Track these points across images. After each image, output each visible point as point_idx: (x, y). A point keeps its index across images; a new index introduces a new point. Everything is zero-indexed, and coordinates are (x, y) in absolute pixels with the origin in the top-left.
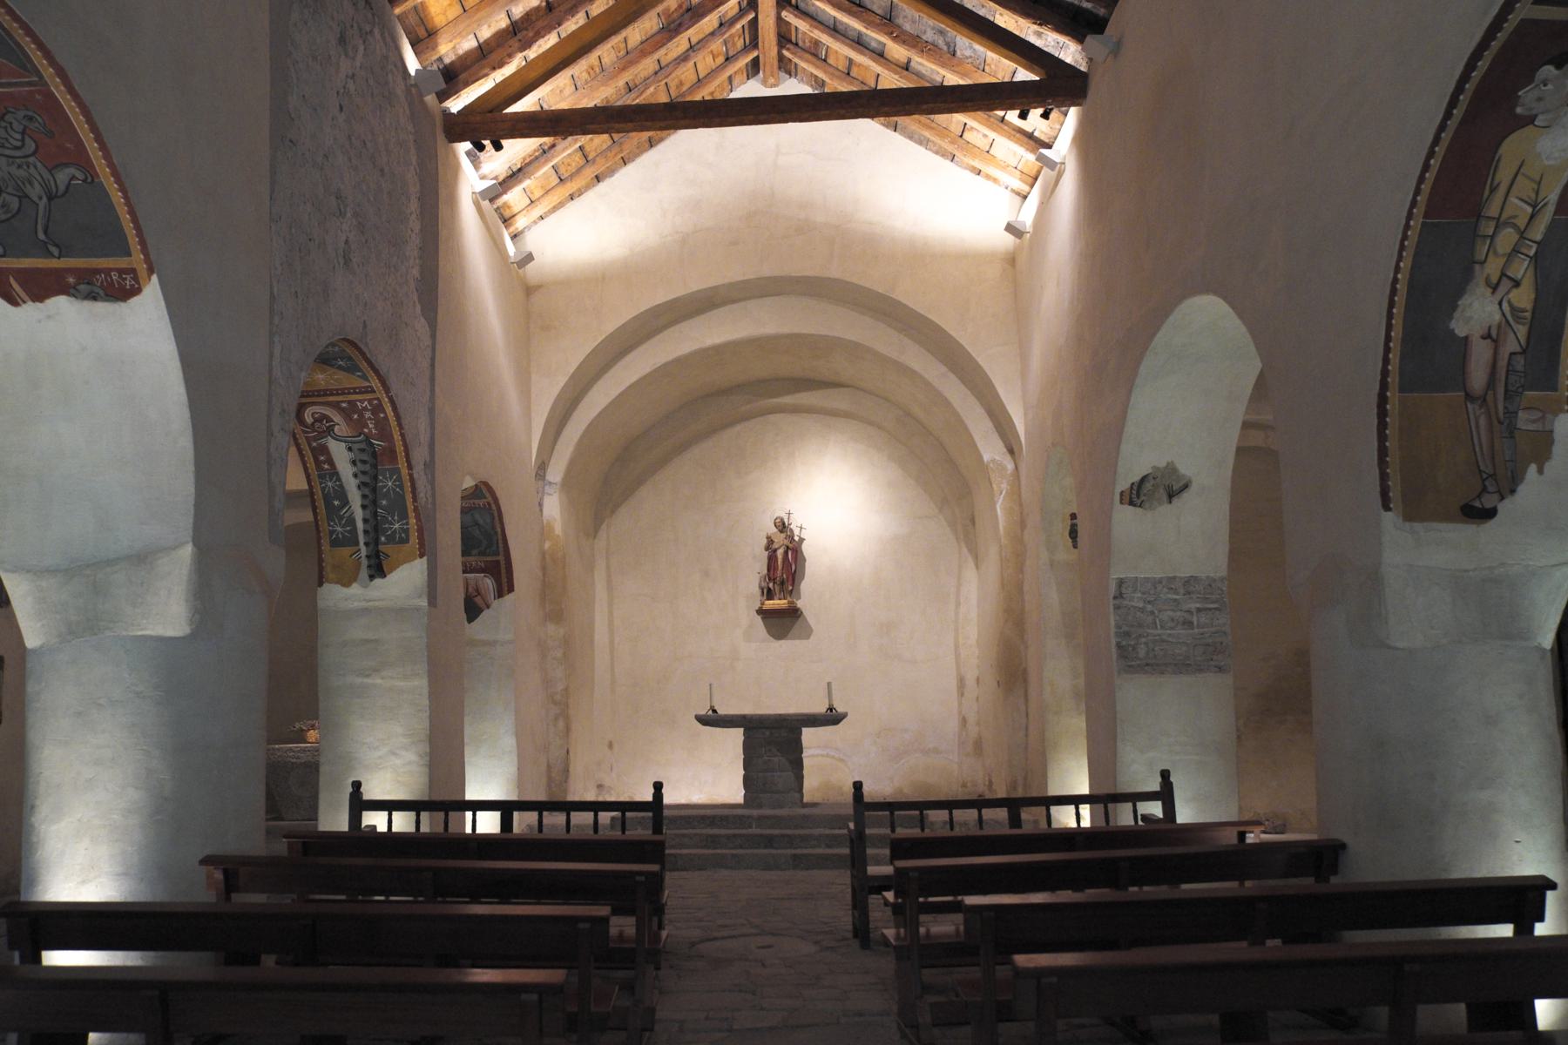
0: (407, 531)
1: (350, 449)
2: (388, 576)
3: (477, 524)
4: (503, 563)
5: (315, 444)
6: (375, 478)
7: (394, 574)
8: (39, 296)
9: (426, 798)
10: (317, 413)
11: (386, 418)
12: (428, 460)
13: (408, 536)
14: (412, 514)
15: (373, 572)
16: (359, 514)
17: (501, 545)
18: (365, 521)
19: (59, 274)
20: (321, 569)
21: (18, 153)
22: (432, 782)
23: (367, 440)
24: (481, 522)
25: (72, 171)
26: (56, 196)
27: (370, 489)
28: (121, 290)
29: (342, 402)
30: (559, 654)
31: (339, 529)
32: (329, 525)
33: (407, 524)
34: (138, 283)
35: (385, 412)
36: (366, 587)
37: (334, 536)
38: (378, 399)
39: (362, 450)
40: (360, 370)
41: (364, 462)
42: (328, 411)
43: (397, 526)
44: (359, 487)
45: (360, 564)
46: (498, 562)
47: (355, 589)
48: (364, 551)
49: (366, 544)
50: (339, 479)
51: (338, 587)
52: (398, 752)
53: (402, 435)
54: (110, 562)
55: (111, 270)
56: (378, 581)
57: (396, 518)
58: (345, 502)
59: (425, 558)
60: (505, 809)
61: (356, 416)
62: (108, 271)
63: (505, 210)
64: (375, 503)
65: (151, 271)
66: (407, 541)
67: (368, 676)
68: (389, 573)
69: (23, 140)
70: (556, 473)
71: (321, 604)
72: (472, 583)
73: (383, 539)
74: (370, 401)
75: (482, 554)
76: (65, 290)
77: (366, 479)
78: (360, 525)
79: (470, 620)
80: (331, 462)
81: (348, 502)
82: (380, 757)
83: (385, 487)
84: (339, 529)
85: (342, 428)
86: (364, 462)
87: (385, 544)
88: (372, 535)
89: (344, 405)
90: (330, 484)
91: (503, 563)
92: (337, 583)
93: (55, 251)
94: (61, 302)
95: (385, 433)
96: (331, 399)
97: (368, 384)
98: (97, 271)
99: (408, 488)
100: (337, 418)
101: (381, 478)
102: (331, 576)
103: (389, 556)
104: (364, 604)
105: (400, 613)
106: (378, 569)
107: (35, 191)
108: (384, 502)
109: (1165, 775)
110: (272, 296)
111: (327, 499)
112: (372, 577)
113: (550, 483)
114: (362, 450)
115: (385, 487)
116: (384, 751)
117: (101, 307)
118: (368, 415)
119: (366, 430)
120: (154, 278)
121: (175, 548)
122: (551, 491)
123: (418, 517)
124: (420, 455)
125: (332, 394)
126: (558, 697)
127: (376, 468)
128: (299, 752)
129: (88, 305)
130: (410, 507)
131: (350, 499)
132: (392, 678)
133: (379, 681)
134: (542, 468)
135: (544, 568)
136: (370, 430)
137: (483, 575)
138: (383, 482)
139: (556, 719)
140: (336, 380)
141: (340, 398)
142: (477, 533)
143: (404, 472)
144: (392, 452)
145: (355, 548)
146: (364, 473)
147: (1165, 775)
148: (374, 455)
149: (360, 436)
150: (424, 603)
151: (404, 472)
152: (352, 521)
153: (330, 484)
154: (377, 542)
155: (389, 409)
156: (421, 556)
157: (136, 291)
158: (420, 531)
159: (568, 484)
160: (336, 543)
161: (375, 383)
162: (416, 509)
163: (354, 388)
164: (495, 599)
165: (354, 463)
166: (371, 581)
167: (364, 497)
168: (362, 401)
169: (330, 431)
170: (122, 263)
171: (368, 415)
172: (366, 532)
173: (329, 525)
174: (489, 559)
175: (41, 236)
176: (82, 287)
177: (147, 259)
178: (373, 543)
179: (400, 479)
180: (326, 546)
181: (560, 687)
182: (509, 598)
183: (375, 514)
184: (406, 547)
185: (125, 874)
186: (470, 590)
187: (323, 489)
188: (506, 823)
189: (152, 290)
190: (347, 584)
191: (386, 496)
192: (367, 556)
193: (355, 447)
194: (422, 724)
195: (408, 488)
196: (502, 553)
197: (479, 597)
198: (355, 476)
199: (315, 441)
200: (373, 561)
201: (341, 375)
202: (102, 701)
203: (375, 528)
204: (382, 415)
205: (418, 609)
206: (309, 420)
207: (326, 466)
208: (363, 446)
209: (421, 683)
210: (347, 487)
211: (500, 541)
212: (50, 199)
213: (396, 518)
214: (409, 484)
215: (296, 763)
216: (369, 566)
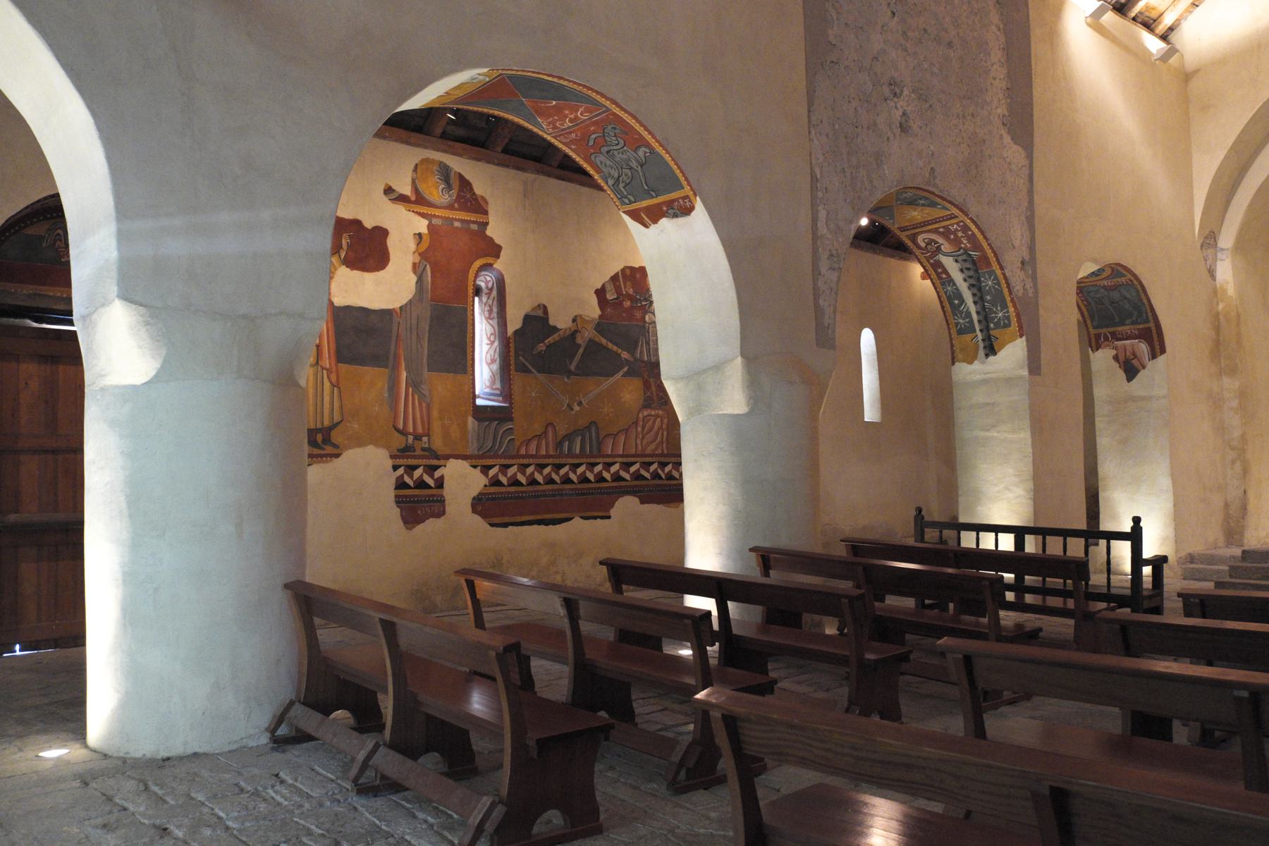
0: (1008, 318)
1: (956, 261)
2: (998, 354)
3: (1125, 298)
4: (1154, 329)
5: (932, 261)
6: (979, 280)
7: (1001, 352)
8: (655, 221)
9: (1032, 525)
10: (926, 239)
11: (973, 234)
12: (1027, 258)
13: (1009, 321)
14: (1010, 305)
15: (987, 352)
17: (1150, 314)
18: (978, 313)
19: (659, 205)
20: (953, 352)
22: (1036, 513)
23: (966, 252)
24: (1128, 296)
25: (643, 149)
26: (644, 165)
27: (977, 287)
28: (687, 211)
29: (940, 228)
30: (1235, 403)
31: (961, 321)
32: (955, 319)
33: (1008, 312)
34: (692, 203)
35: (970, 230)
36: (983, 363)
37: (959, 327)
38: (962, 221)
39: (965, 260)
40: (940, 204)
41: (968, 269)
42: (934, 237)
43: (1000, 315)
44: (969, 288)
45: (978, 346)
46: (1149, 329)
47: (976, 365)
48: (980, 337)
49: (981, 331)
50: (955, 284)
52: (1010, 487)
53: (989, 245)
54: (705, 371)
55: (680, 198)
56: (991, 358)
57: (999, 308)
58: (962, 301)
59: (1024, 338)
60: (1019, 533)
61: (952, 237)
62: (676, 200)
63: (1150, 13)
64: (982, 298)
65: (695, 195)
66: (1009, 325)
67: (988, 430)
68: (999, 351)
69: (617, 140)
70: (1227, 239)
71: (955, 378)
73: (992, 325)
74: (957, 224)
75: (1133, 323)
76: (664, 215)
77: (973, 282)
78: (975, 317)
79: (1129, 379)
81: (963, 301)
82: (998, 492)
83: (987, 285)
84: (961, 321)
85: (946, 247)
86: (968, 269)
87: (994, 329)
88: (984, 323)
89: (941, 230)
90: (949, 288)
91: (1154, 329)
92: (964, 361)
94: (664, 222)
95: (977, 246)
96: (930, 227)
97: (950, 213)
98: (672, 201)
100: (941, 240)
101: (983, 279)
102: (960, 356)
103: (997, 339)
104: (984, 377)
105: (1009, 381)
106: (991, 350)
107: (634, 164)
108: (988, 298)
109: (1137, 520)
110: (814, 179)
111: (950, 299)
112: (987, 356)
113: (1222, 250)
114: (965, 260)
115: (987, 285)
116: (1001, 486)
117: (681, 220)
118: (960, 234)
119: (963, 246)
120: (698, 198)
121: (733, 359)
122: (1224, 257)
123: (1015, 306)
124: (1012, 260)
125: (944, 220)
126: (1235, 443)
127: (978, 273)
129: (675, 220)
130: (1008, 299)
131: (965, 298)
132: (1005, 431)
133: (996, 434)
134: (1210, 239)
135: (1217, 329)
136: (965, 244)
137: (1137, 340)
138: (985, 282)
139: (1233, 462)
140: (927, 214)
141: (936, 226)
142: (1127, 306)
143: (999, 272)
144: (985, 258)
145: (974, 335)
146: (970, 277)
147: (1137, 520)
148: (974, 262)
149: (959, 250)
150: (1025, 373)
151: (999, 272)
152: (968, 314)
153: (949, 288)
154: (988, 328)
155: (973, 227)
156: (1021, 336)
157: (692, 209)
158: (1018, 316)
159: (1241, 246)
160: (960, 332)
161: (955, 211)
162: (1012, 300)
163: (943, 217)
165: (962, 270)
166: (987, 358)
167: (974, 295)
168: (952, 225)
169: (939, 249)
170: (674, 195)
171: (960, 234)
172: (979, 321)
173: (955, 319)
174: (1141, 326)
175: (646, 188)
176: (670, 211)
177: (692, 189)
178: (986, 330)
179: (996, 278)
180: (954, 335)
181: (1237, 434)
182: (1161, 359)
183: (984, 308)
185: (721, 554)
186: (1128, 353)
187: (946, 293)
188: (1019, 543)
189: (699, 205)
190: (970, 362)
191: (989, 293)
192: (983, 340)
193: (960, 259)
194: (1027, 467)
196: (1152, 321)
197: (1136, 359)
198: (965, 280)
199: (932, 258)
200: (987, 344)
201: (927, 210)
202: (705, 453)
203: (985, 318)
204: (970, 233)
205: (1021, 377)
206: (923, 245)
207: (944, 276)
208: (964, 257)
209: (1025, 436)
210: (961, 289)
211: (1149, 311)
212: (641, 166)
213: (999, 308)
214: (1004, 281)
216: (985, 347)
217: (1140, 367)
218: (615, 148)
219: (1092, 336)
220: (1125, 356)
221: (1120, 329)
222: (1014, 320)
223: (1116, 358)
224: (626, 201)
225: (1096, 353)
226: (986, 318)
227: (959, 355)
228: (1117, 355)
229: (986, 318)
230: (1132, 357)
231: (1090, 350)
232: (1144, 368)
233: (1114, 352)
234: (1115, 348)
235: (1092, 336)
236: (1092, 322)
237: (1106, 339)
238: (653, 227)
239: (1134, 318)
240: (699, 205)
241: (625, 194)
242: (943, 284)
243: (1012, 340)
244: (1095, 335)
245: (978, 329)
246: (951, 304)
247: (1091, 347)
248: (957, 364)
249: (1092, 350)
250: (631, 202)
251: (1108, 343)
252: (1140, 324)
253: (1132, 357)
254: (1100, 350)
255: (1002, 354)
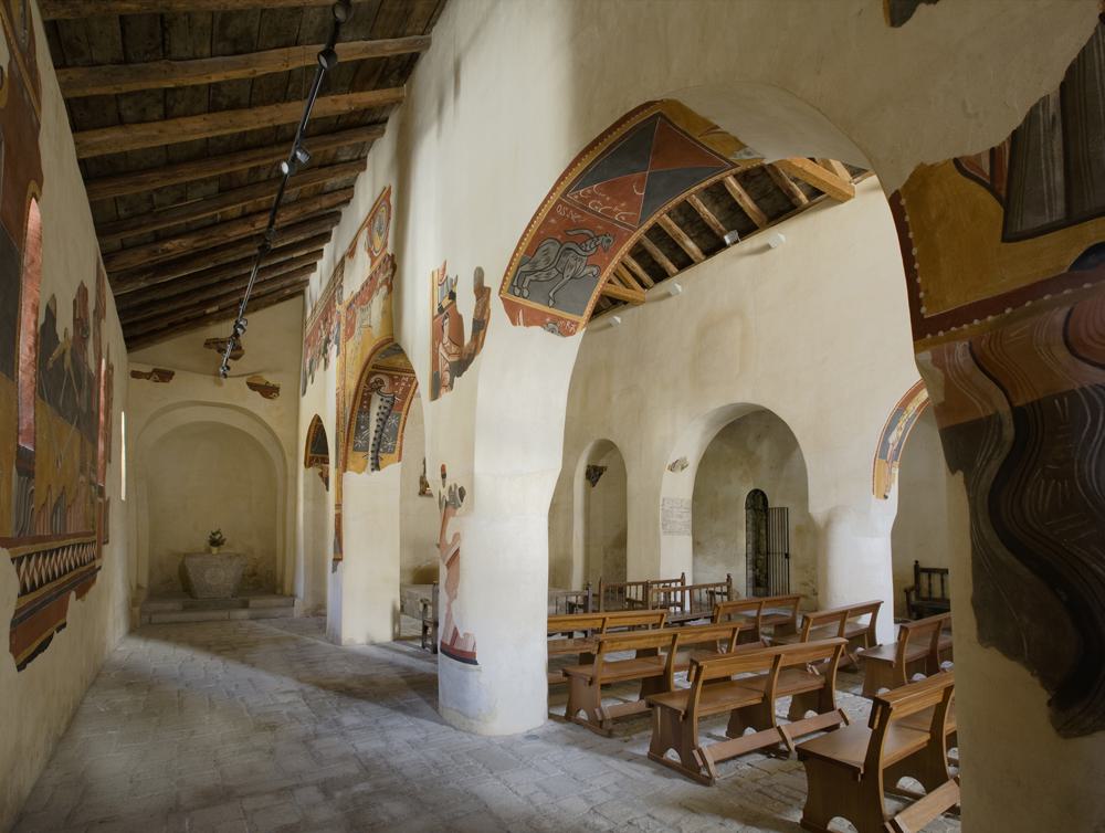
6: (387, 417)
8: (527, 324)
14: (399, 438)
16: (372, 434)
18: (375, 439)
19: (545, 314)
21: (583, 253)
28: (565, 332)
51: (355, 474)
56: (375, 472)
58: (368, 428)
76: (543, 324)
77: (382, 417)
80: (368, 405)
86: (385, 408)
93: (551, 303)
94: (537, 330)
98: (562, 319)
99: (401, 425)
106: (376, 467)
112: (373, 470)
117: (554, 337)
130: (399, 435)
141: (393, 373)
143: (403, 416)
151: (403, 416)
152: (367, 439)
154: (378, 451)
157: (572, 334)
160: (355, 450)
175: (551, 294)
178: (376, 452)
179: (399, 420)
180: (351, 448)
184: (392, 456)
195: (401, 425)
208: (389, 399)
218: (580, 252)
222: (397, 452)
224: (517, 292)
226: (379, 443)
227: (350, 465)
229: (379, 443)
237: (317, 461)
238: (521, 329)
240: (580, 334)
241: (525, 285)
242: (360, 412)
243: (393, 462)
245: (370, 449)
246: (358, 427)
248: (348, 472)
250: (521, 295)
255: (382, 471)
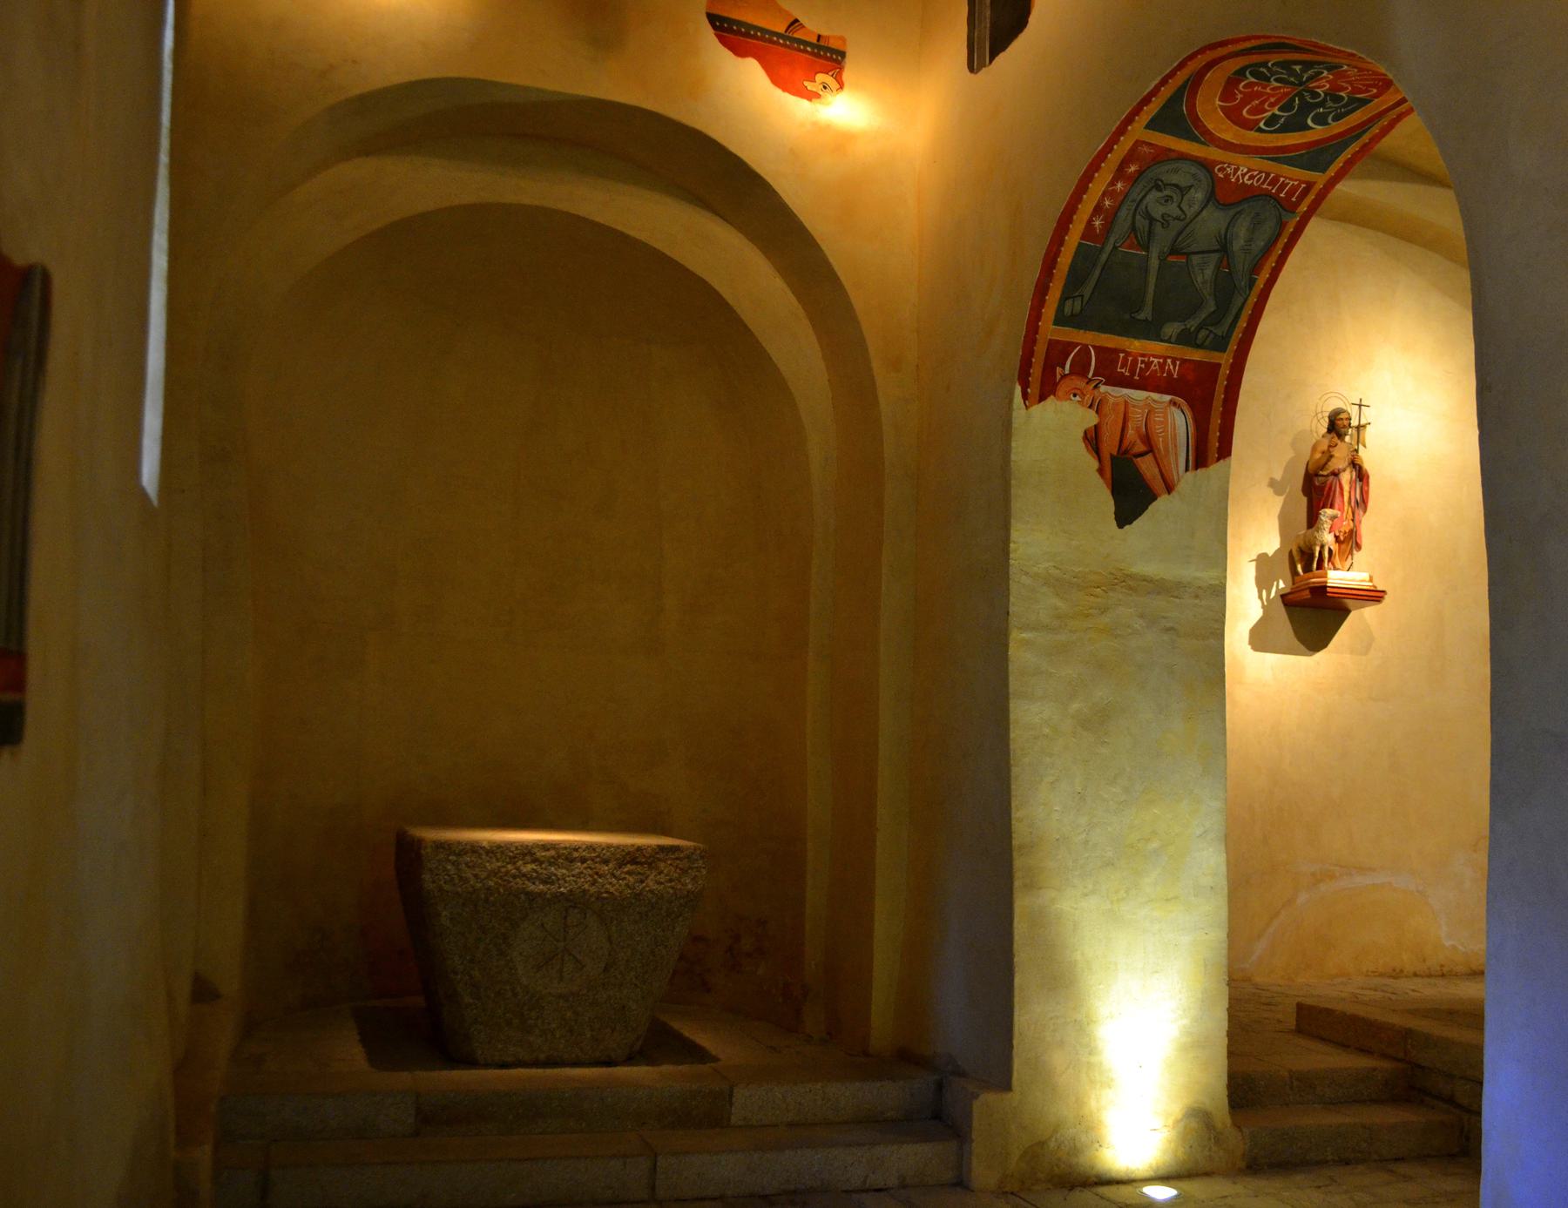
4: (1225, 371)
72: (1137, 417)
75: (1186, 339)
128: (553, 862)
137: (1167, 398)
164: (1187, 470)
174: (1197, 355)
186: (1131, 433)
197: (1149, 457)
215: (541, 894)
217: (1158, 484)
219: (1040, 350)
220: (1121, 441)
221: (1136, 345)
223: (1093, 439)
225: (1037, 409)
228: (1096, 427)
230: (1141, 448)
231: (1018, 390)
232: (1169, 489)
233: (1091, 419)
234: (1098, 406)
235: (1040, 350)
236: (1064, 299)
237: (1080, 369)
239: (1192, 324)
244: (1052, 344)
247: (1025, 386)
249: (1025, 396)
251: (1080, 383)
252: (1199, 346)
253: (1141, 448)
254: (1051, 401)
